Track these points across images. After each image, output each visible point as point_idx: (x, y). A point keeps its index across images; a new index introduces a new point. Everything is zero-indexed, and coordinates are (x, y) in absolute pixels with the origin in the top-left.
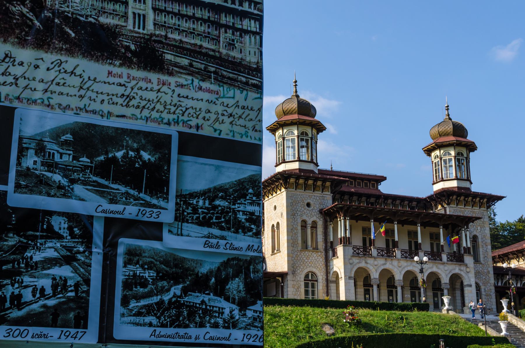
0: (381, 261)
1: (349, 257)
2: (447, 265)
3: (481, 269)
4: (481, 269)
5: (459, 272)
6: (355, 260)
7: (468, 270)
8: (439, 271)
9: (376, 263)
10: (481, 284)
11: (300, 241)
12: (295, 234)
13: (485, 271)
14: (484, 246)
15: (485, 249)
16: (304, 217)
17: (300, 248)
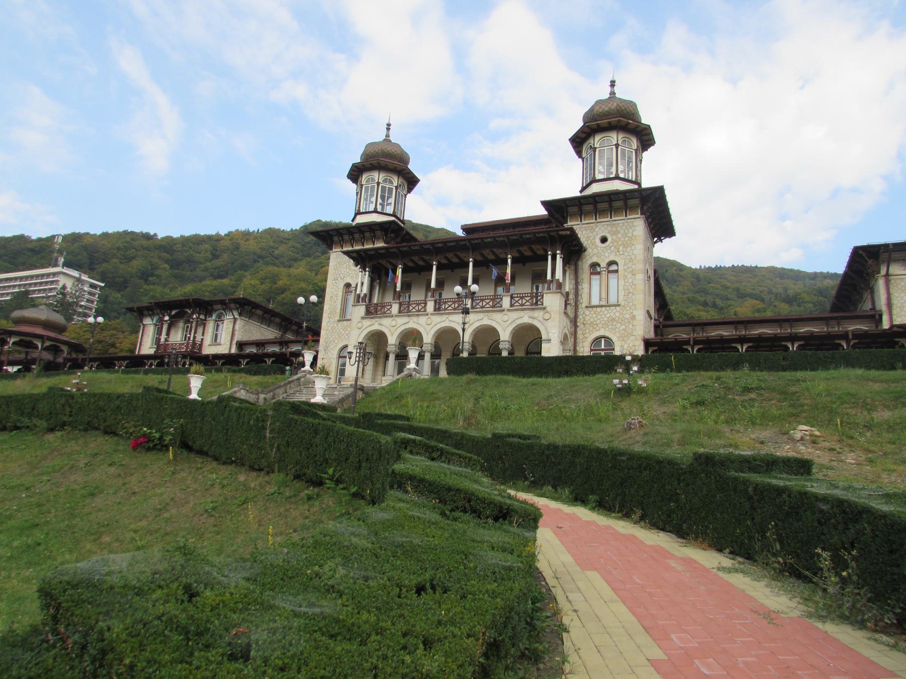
0: (402, 320)
1: (359, 319)
2: (509, 313)
3: (617, 314)
4: (617, 314)
5: (530, 321)
6: (367, 322)
7: (547, 316)
8: (494, 324)
9: (394, 323)
10: (614, 339)
11: (338, 310)
12: (335, 302)
13: (627, 316)
14: (629, 276)
15: (630, 281)
16: (348, 280)
17: (338, 318)
